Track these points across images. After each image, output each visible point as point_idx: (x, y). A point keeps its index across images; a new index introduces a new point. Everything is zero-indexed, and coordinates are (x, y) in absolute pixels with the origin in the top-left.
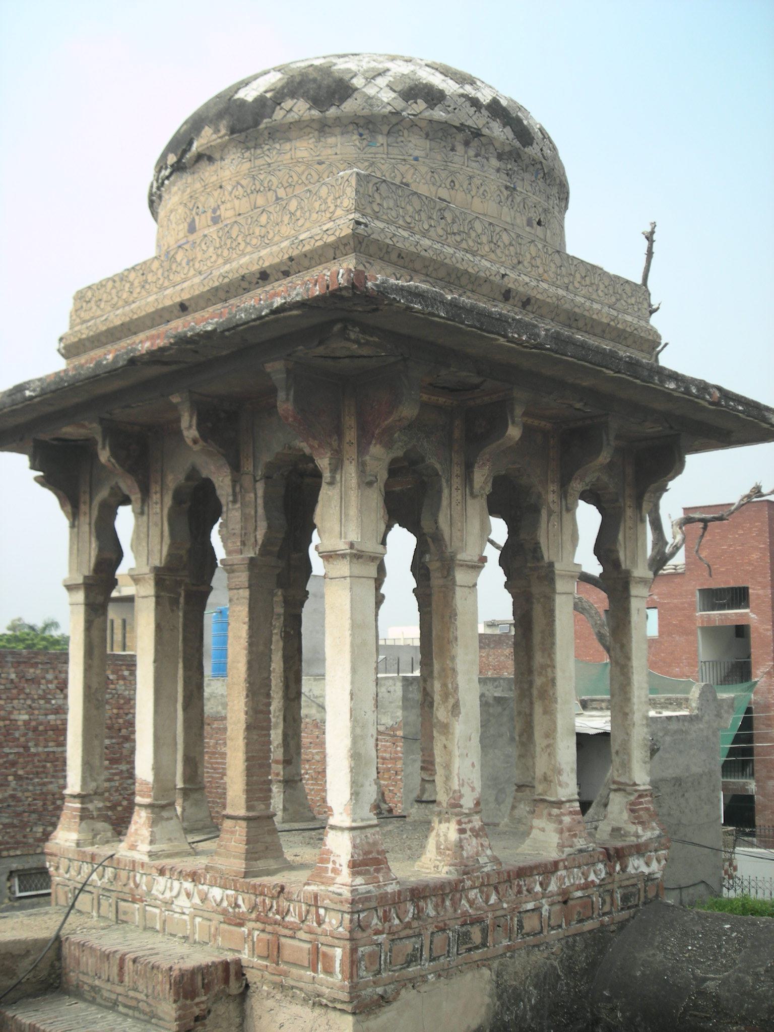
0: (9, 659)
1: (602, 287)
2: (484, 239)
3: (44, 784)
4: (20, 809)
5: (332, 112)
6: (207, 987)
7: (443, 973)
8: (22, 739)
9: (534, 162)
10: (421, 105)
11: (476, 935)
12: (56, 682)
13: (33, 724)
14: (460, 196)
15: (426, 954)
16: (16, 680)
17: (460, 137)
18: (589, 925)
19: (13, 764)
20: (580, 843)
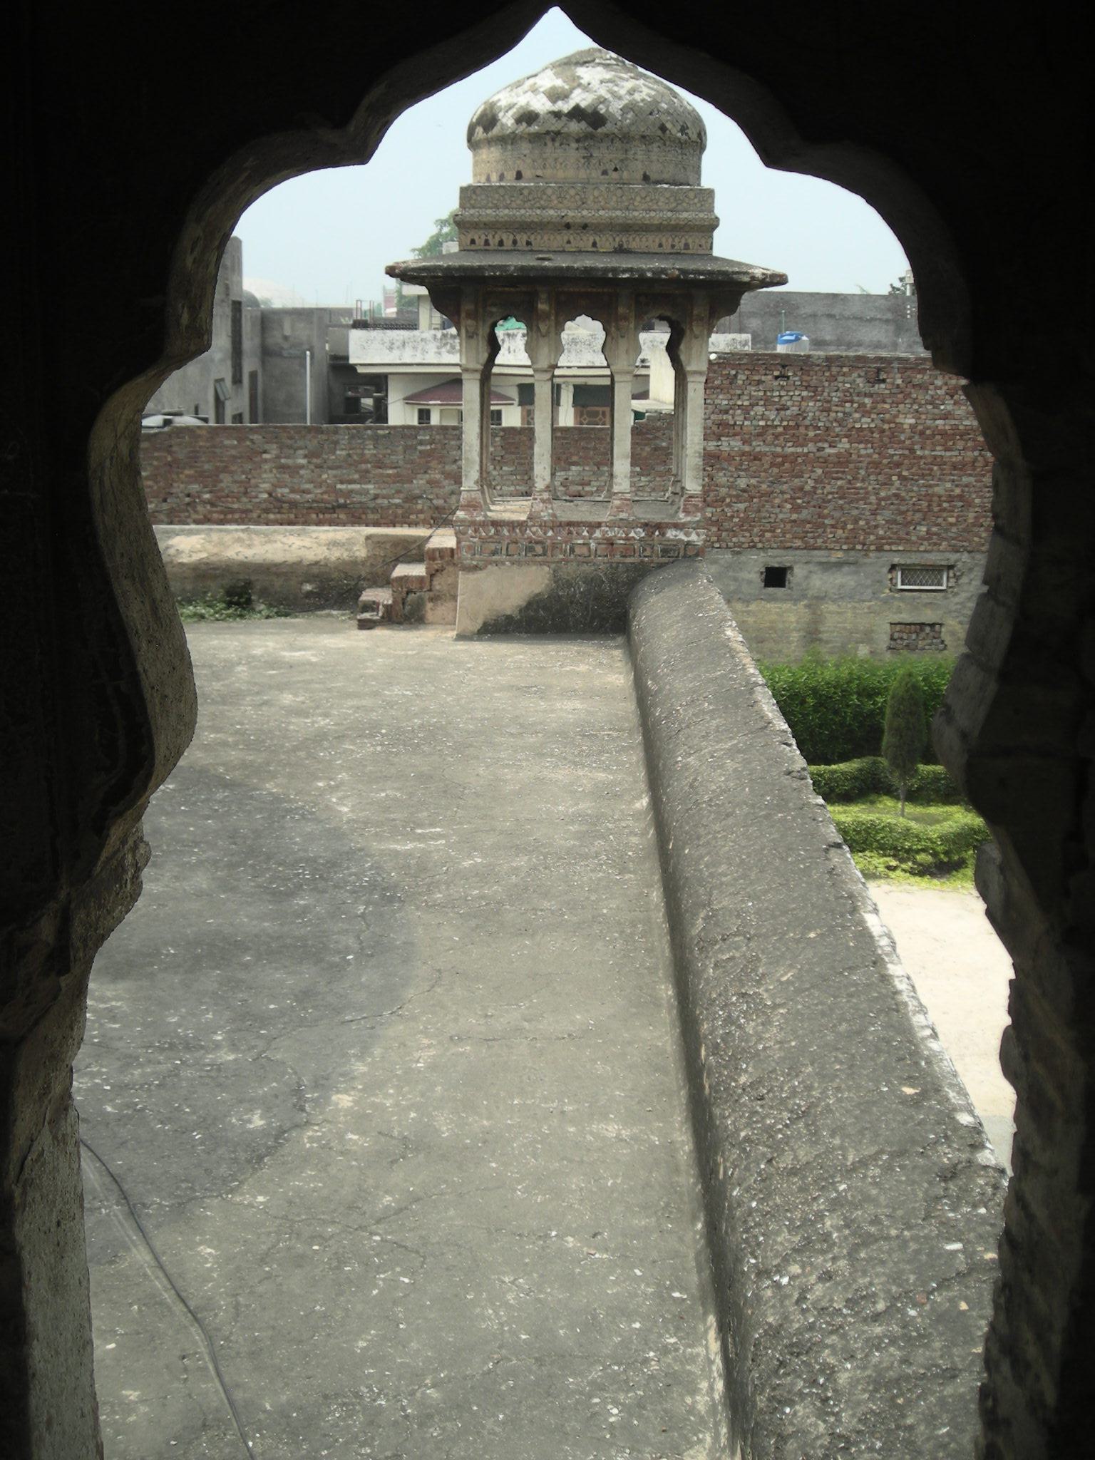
0: (896, 365)
1: (662, 199)
2: (554, 197)
3: (930, 486)
4: (903, 508)
5: (490, 134)
6: (442, 557)
7: (519, 563)
8: (908, 442)
9: (607, 135)
10: (524, 124)
11: (539, 549)
12: (945, 388)
13: (920, 427)
14: (548, 172)
15: (504, 552)
16: (902, 385)
17: (548, 137)
18: (629, 560)
19: (898, 465)
20: (623, 515)
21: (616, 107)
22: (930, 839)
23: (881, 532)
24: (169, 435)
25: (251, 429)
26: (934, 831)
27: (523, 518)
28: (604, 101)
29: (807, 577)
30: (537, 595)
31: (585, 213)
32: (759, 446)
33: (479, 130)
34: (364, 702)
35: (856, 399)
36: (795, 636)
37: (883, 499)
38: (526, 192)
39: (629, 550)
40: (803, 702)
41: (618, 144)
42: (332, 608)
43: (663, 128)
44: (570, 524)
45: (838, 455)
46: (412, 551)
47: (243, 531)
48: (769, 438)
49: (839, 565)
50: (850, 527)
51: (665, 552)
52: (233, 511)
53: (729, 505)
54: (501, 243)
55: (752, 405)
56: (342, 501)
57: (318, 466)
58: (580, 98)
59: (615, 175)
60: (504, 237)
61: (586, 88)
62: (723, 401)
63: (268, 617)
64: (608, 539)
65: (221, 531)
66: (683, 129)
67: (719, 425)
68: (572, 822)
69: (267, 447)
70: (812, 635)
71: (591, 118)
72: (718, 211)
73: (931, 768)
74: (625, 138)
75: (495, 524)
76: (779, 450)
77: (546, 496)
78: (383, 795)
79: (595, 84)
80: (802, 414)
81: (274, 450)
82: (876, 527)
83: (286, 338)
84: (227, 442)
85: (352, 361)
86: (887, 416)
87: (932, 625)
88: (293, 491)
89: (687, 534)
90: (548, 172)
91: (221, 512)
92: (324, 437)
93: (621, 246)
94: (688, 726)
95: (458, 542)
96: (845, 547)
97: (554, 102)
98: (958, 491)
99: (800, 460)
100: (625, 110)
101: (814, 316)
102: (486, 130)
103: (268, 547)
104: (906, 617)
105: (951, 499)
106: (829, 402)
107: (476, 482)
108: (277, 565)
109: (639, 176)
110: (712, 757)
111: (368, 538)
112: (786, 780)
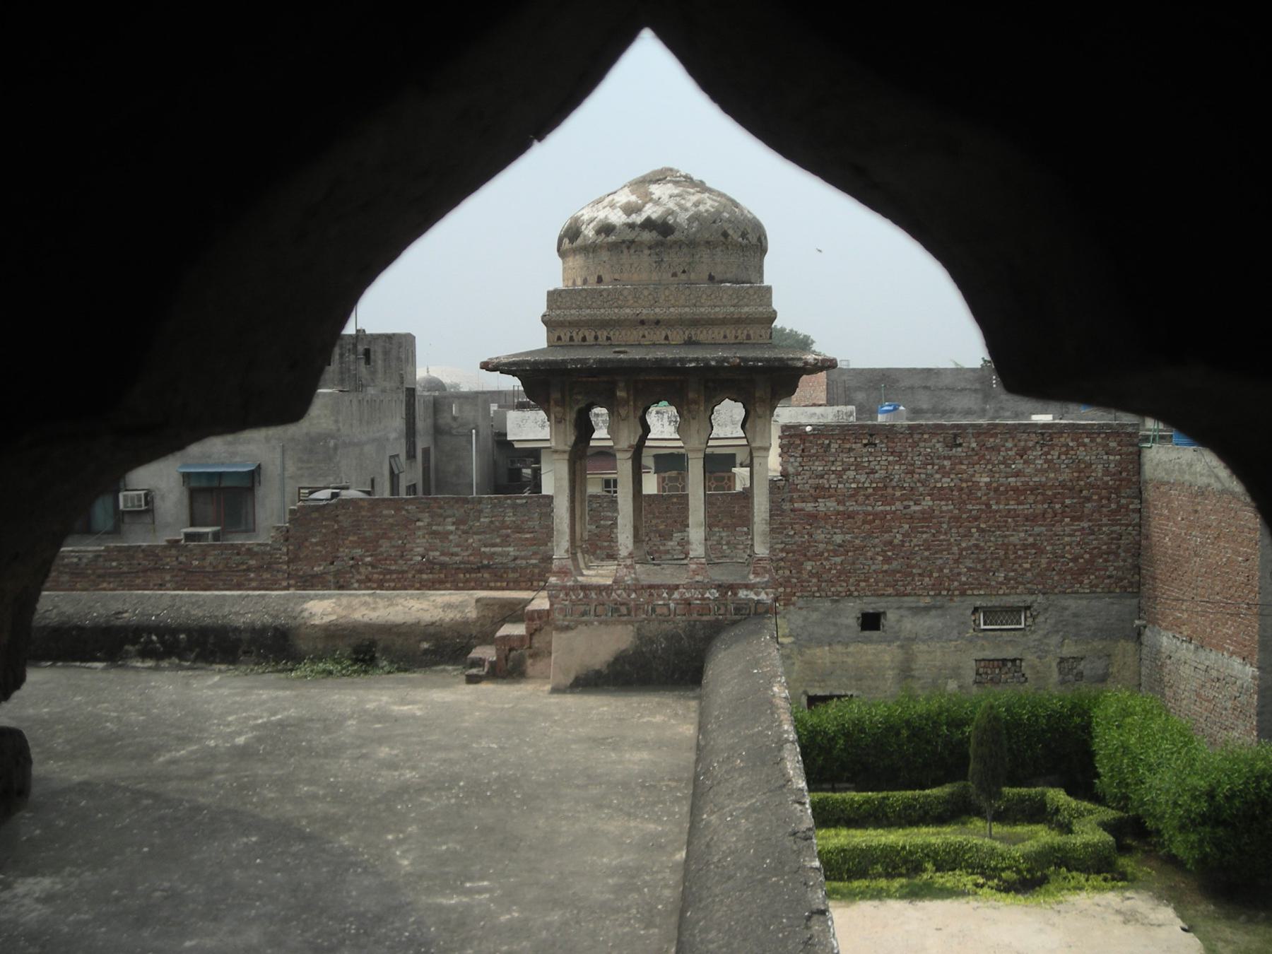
0: (970, 431)
3: (1006, 536)
4: (983, 557)
6: (540, 618)
7: (606, 623)
8: (984, 498)
9: (675, 242)
11: (624, 610)
13: (995, 485)
14: (625, 276)
16: (977, 448)
18: (705, 618)
19: (977, 519)
20: (698, 578)
21: (683, 218)
22: (1014, 858)
23: (964, 579)
24: (336, 506)
25: (406, 500)
26: (1017, 851)
27: (609, 582)
29: (899, 621)
30: (624, 651)
31: (657, 310)
32: (852, 506)
33: (566, 241)
34: (452, 755)
35: (936, 461)
37: (965, 549)
38: (605, 294)
39: (705, 608)
40: (898, 734)
41: (685, 250)
42: (447, 663)
43: (725, 235)
44: (651, 587)
45: (923, 512)
46: (514, 612)
47: (369, 595)
48: (861, 498)
49: (927, 609)
50: (935, 575)
51: (738, 610)
52: (391, 572)
53: (827, 559)
54: (584, 339)
55: (845, 470)
56: (486, 562)
57: (465, 532)
58: (651, 211)
59: (684, 277)
60: (587, 333)
61: (657, 202)
63: (389, 672)
64: (686, 600)
65: (350, 595)
66: (744, 235)
67: (816, 489)
68: (612, 875)
69: (420, 515)
70: (906, 672)
71: (661, 227)
72: (775, 306)
73: (1015, 790)
74: (691, 244)
75: (585, 588)
76: (870, 508)
77: (629, 562)
78: (444, 847)
79: (665, 198)
80: (889, 477)
81: (426, 519)
82: (959, 574)
83: (455, 419)
84: (385, 512)
85: (509, 438)
86: (965, 476)
87: (1014, 661)
88: (443, 554)
89: (757, 594)
90: (625, 276)
91: (380, 573)
92: (470, 506)
93: (690, 338)
94: (719, 783)
95: (551, 605)
96: (932, 593)
97: (629, 215)
98: (1031, 540)
99: (888, 517)
100: (691, 220)
101: (912, 388)
102: (572, 241)
103: (391, 609)
105: (1025, 547)
106: (912, 465)
107: (567, 551)
108: (398, 626)
109: (706, 276)
110: (731, 815)
111: (478, 600)
112: (789, 842)
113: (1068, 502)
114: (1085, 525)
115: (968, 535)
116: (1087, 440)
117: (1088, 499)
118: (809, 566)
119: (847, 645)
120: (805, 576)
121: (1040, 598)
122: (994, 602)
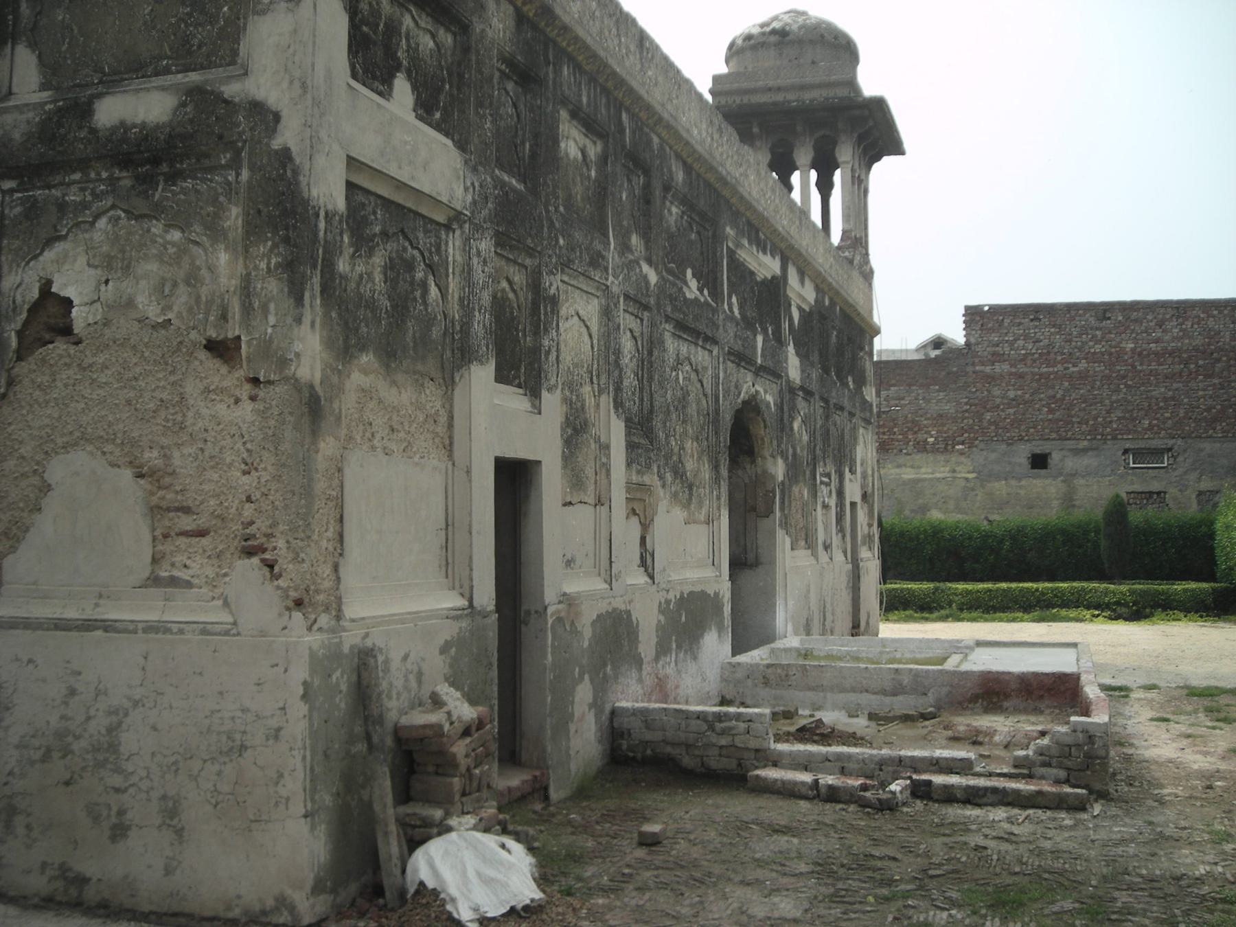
4: (1130, 408)
19: (1124, 377)
21: (795, 27)
28: (786, 24)
29: (1062, 460)
32: (1022, 369)
36: (1055, 503)
43: (822, 36)
45: (1079, 372)
48: (1029, 362)
49: (1085, 450)
53: (1003, 410)
55: (1015, 340)
62: (995, 338)
70: (1068, 501)
80: (1051, 345)
82: (1111, 422)
87: (1159, 493)
100: (800, 28)
104: (1138, 487)
105: (1165, 400)
113: (1201, 362)
114: (1216, 381)
115: (1118, 390)
116: (1215, 312)
117: (1219, 360)
118: (988, 416)
119: (1020, 480)
120: (985, 424)
121: (1180, 442)
122: (1141, 444)
